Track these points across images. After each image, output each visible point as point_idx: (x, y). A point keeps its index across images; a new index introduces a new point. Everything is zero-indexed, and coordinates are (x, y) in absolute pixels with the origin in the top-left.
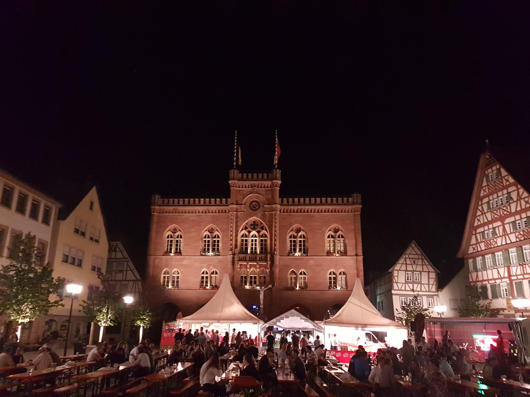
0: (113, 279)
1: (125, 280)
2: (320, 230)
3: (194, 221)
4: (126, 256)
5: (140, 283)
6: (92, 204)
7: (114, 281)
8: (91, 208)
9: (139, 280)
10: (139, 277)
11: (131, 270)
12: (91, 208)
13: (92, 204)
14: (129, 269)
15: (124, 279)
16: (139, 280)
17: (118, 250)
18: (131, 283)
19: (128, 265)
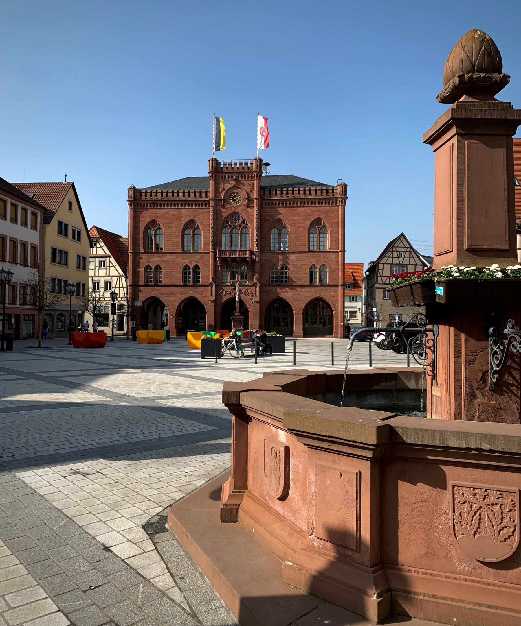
0: (96, 275)
1: (109, 276)
2: (302, 223)
3: (173, 215)
4: (108, 252)
5: (123, 279)
6: (70, 203)
7: (98, 276)
8: (70, 208)
9: (122, 276)
10: (122, 273)
11: (114, 266)
12: (70, 208)
13: (70, 203)
14: (111, 265)
15: (107, 275)
16: (122, 276)
17: (98, 245)
18: (115, 279)
19: (110, 261)
